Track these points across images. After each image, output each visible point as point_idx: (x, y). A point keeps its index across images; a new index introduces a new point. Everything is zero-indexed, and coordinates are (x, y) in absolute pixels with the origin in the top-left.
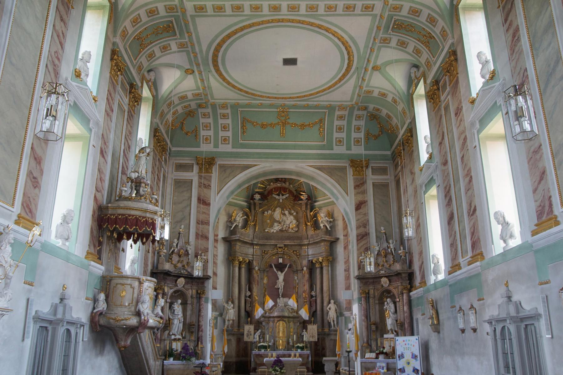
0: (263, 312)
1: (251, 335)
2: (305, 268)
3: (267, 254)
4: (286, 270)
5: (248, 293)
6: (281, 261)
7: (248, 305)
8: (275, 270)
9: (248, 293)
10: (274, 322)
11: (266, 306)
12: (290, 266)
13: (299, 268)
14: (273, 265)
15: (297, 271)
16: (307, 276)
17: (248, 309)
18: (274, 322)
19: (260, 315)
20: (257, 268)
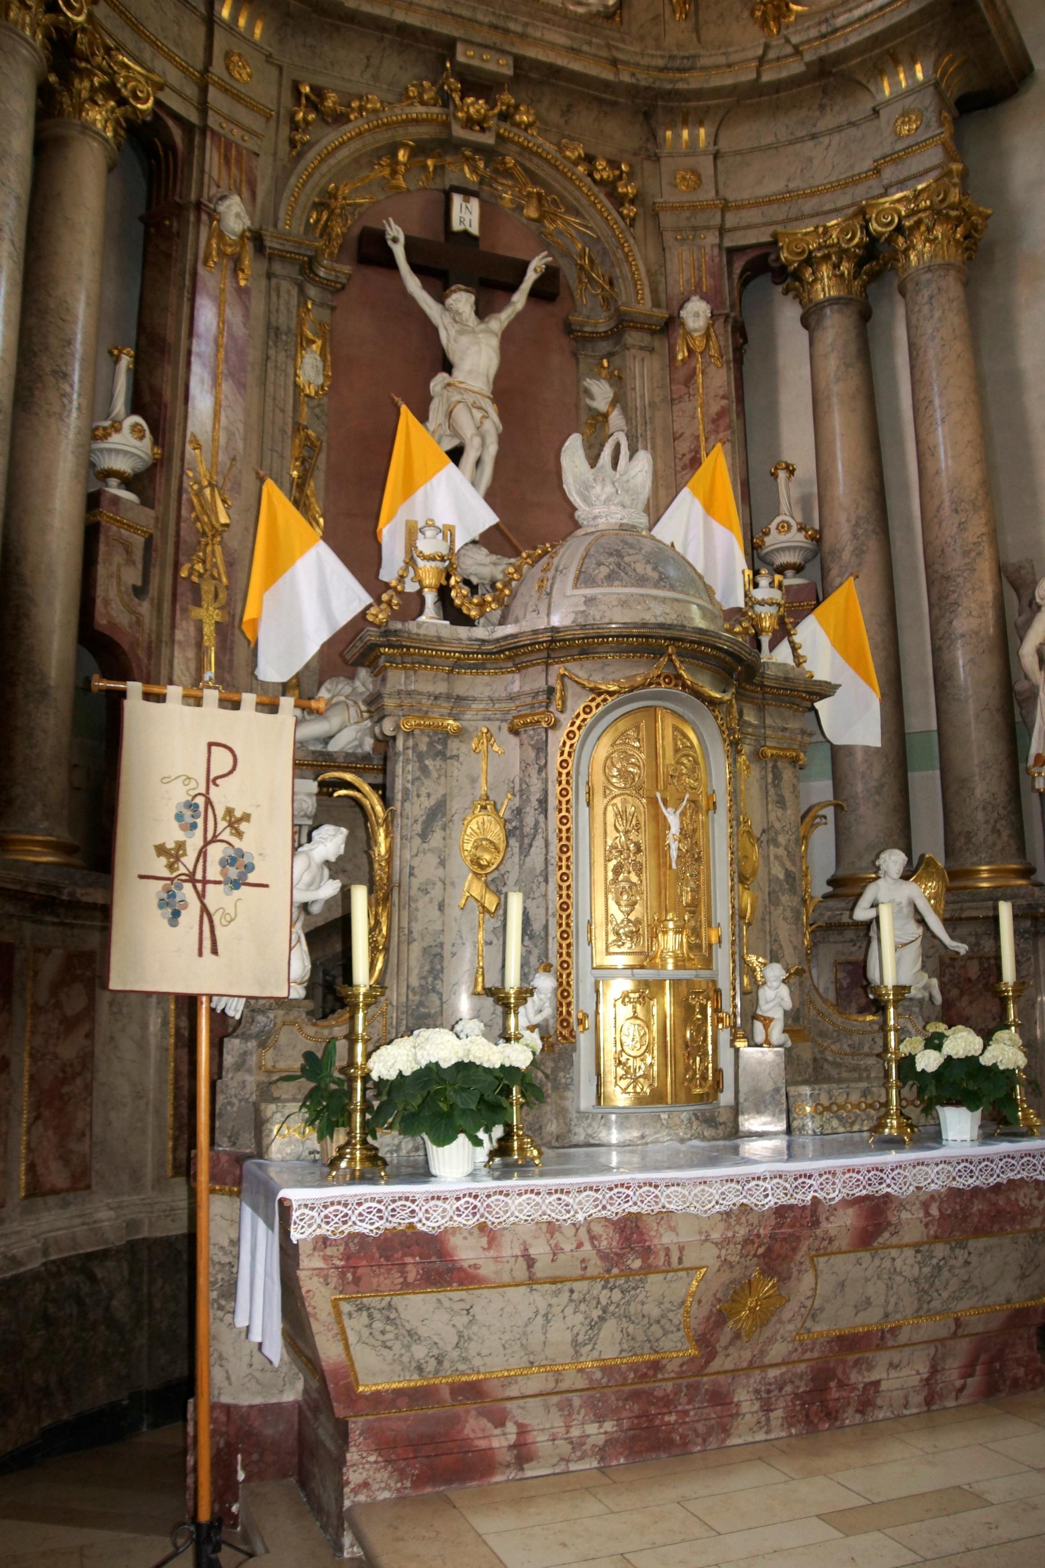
0: (349, 598)
1: (239, 872)
2: (696, 314)
3: (340, 119)
4: (519, 299)
5: (128, 446)
6: (466, 215)
7: (117, 575)
8: (413, 284)
9: (128, 446)
10: (529, 723)
11: (391, 536)
12: (546, 291)
13: (642, 305)
14: (396, 233)
15: (623, 324)
16: (715, 380)
17: (114, 609)
18: (529, 723)
19: (312, 648)
20: (235, 215)
